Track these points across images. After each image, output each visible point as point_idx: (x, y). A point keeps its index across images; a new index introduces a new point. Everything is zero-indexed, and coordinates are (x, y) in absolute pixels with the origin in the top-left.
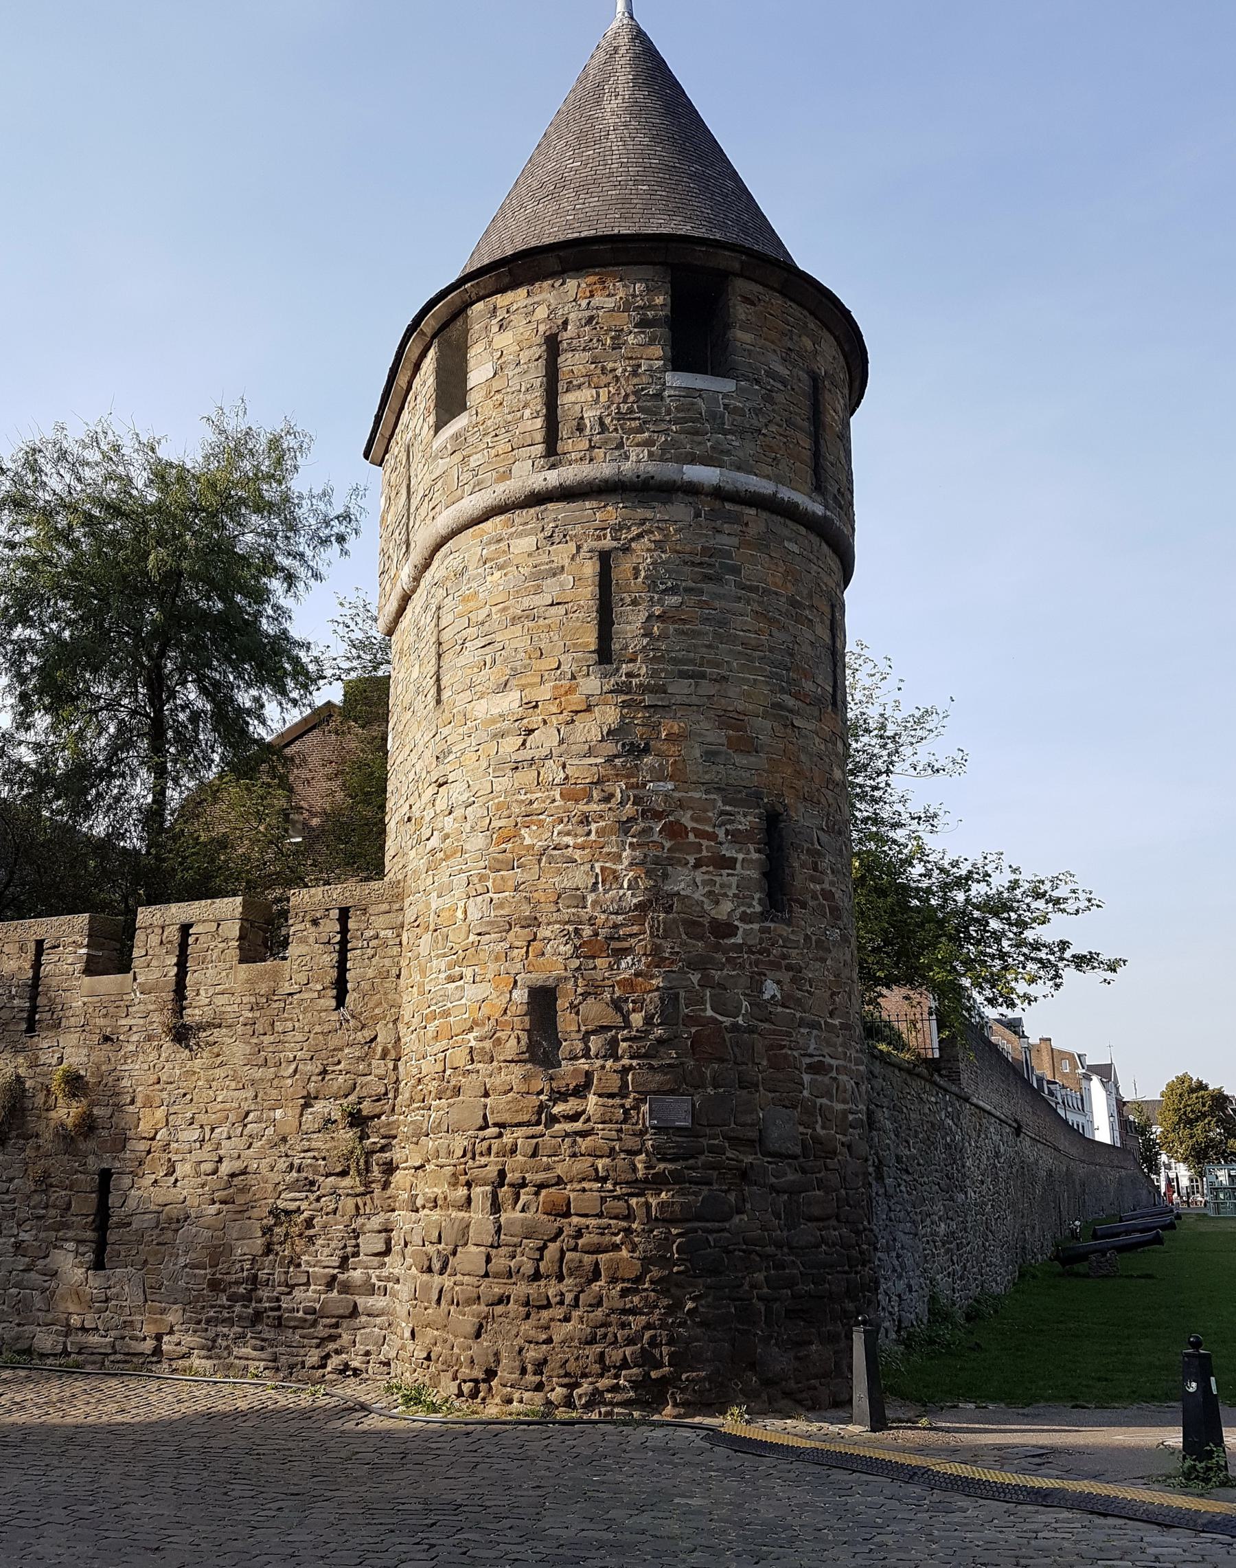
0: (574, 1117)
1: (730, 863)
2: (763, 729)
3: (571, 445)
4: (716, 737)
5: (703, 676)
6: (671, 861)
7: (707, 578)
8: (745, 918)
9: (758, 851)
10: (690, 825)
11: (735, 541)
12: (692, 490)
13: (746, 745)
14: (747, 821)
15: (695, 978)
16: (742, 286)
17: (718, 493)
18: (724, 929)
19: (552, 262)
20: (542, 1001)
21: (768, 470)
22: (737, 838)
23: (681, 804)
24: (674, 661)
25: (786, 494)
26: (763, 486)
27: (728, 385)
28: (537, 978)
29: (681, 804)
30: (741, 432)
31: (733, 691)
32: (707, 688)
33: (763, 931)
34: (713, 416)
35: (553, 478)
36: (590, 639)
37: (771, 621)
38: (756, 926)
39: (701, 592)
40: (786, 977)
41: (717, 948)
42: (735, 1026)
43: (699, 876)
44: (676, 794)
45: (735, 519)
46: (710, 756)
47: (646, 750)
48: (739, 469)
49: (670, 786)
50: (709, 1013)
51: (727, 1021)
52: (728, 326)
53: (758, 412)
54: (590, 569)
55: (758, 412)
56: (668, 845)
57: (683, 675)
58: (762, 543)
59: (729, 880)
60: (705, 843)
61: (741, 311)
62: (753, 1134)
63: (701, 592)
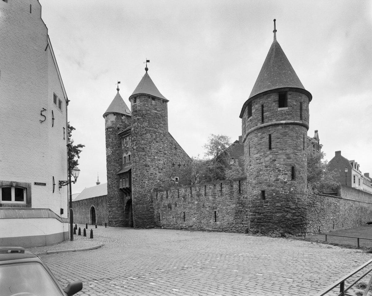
0: (267, 205)
1: (287, 174)
2: (292, 155)
3: (265, 120)
4: (285, 157)
5: (283, 150)
6: (279, 175)
7: (284, 136)
8: (289, 181)
9: (291, 172)
10: (281, 170)
11: (288, 130)
12: (282, 124)
13: (288, 158)
14: (290, 168)
15: (282, 189)
16: (289, 92)
17: (286, 124)
18: (286, 183)
19: (262, 94)
20: (263, 192)
21: (293, 119)
22: (288, 171)
23: (280, 167)
24: (279, 148)
25: (296, 122)
26: (293, 121)
27: (287, 108)
28: (263, 189)
29: (280, 167)
30: (288, 115)
31: (288, 151)
32: (284, 151)
33: (291, 182)
34: (285, 113)
35: (263, 125)
36: (268, 146)
37: (293, 140)
38: (290, 182)
39: (283, 138)
40: (294, 188)
41: (285, 185)
42: (287, 195)
43: (282, 176)
44: (280, 166)
45: (288, 127)
46: (284, 160)
47: (275, 160)
48: (288, 120)
49: (279, 165)
50: (283, 193)
51: (286, 194)
52: (287, 99)
53: (291, 111)
54: (268, 137)
55: (291, 111)
56: (278, 172)
57: (280, 150)
58: (292, 130)
59: (287, 176)
60: (283, 172)
61: (289, 96)
62: (289, 207)
63: (283, 138)
